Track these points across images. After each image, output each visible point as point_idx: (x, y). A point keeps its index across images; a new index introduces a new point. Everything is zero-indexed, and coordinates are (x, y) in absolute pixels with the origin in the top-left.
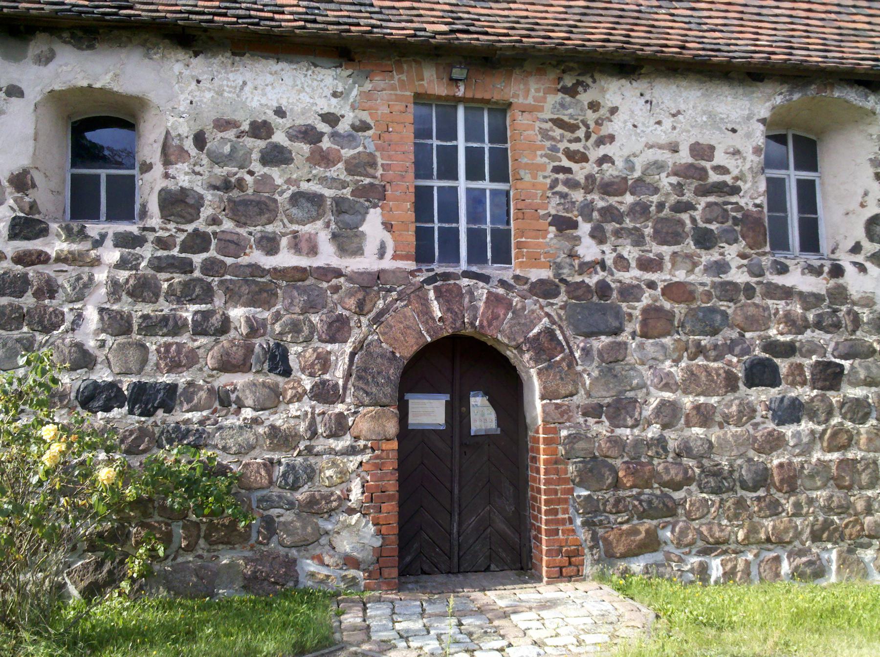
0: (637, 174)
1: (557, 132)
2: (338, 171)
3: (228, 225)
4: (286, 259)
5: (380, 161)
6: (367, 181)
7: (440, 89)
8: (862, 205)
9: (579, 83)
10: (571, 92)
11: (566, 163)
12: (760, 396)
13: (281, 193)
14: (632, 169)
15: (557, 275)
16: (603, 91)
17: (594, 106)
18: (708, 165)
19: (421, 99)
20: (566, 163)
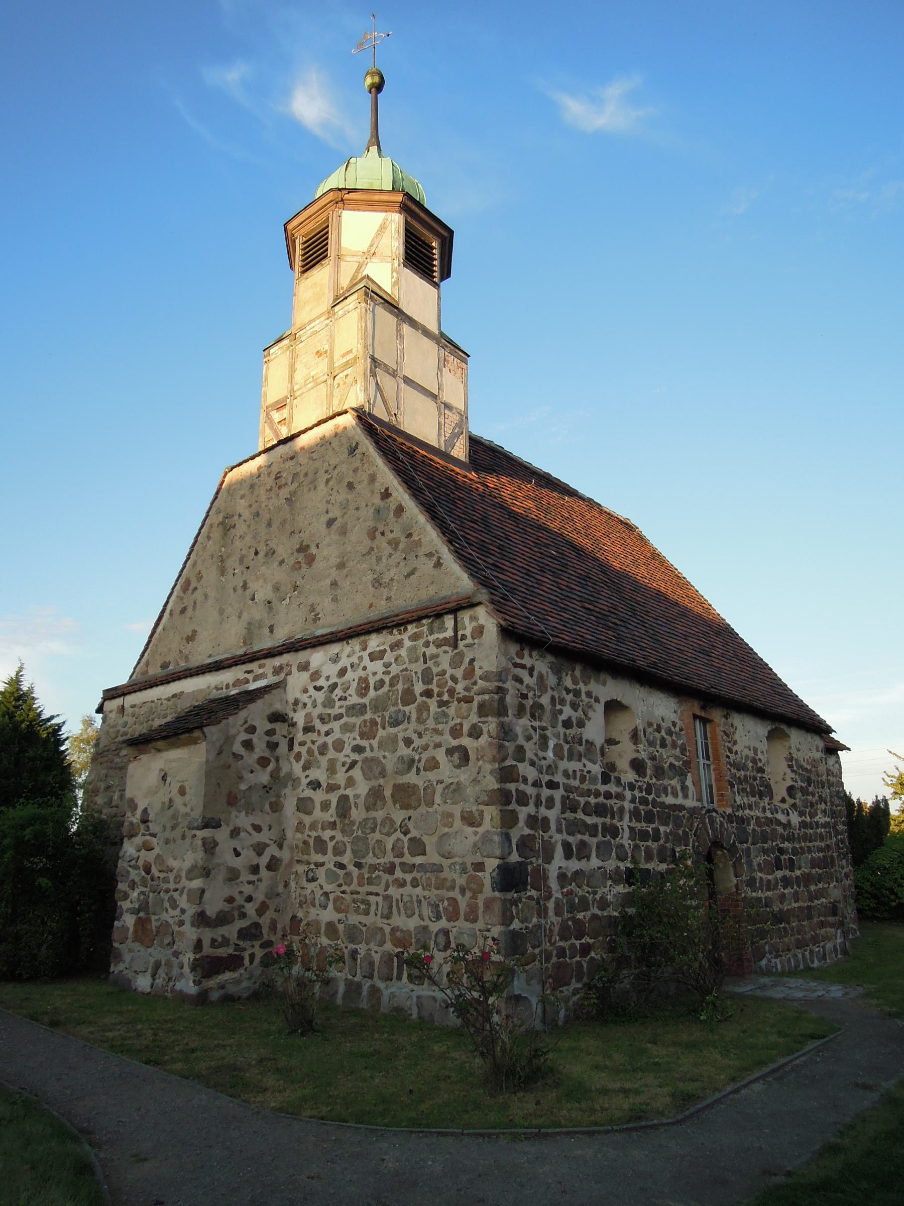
0: (743, 761)
1: (725, 737)
2: (677, 752)
3: (654, 780)
4: (669, 800)
5: (688, 748)
6: (685, 758)
7: (698, 713)
8: (784, 780)
9: (727, 713)
10: (726, 717)
11: (728, 753)
12: (779, 874)
13: (666, 763)
14: (742, 758)
15: (733, 811)
16: (733, 718)
17: (732, 725)
18: (757, 758)
19: (695, 717)
20: (728, 753)
